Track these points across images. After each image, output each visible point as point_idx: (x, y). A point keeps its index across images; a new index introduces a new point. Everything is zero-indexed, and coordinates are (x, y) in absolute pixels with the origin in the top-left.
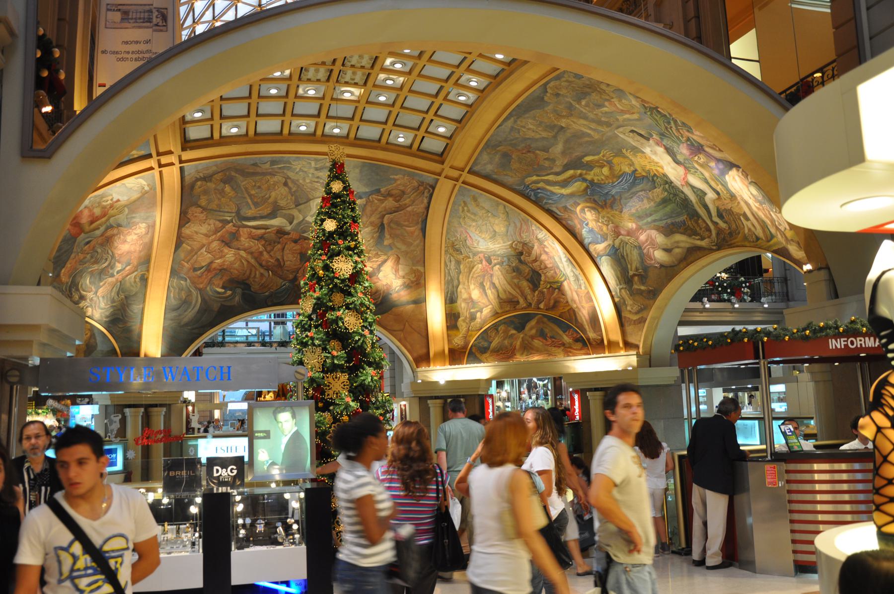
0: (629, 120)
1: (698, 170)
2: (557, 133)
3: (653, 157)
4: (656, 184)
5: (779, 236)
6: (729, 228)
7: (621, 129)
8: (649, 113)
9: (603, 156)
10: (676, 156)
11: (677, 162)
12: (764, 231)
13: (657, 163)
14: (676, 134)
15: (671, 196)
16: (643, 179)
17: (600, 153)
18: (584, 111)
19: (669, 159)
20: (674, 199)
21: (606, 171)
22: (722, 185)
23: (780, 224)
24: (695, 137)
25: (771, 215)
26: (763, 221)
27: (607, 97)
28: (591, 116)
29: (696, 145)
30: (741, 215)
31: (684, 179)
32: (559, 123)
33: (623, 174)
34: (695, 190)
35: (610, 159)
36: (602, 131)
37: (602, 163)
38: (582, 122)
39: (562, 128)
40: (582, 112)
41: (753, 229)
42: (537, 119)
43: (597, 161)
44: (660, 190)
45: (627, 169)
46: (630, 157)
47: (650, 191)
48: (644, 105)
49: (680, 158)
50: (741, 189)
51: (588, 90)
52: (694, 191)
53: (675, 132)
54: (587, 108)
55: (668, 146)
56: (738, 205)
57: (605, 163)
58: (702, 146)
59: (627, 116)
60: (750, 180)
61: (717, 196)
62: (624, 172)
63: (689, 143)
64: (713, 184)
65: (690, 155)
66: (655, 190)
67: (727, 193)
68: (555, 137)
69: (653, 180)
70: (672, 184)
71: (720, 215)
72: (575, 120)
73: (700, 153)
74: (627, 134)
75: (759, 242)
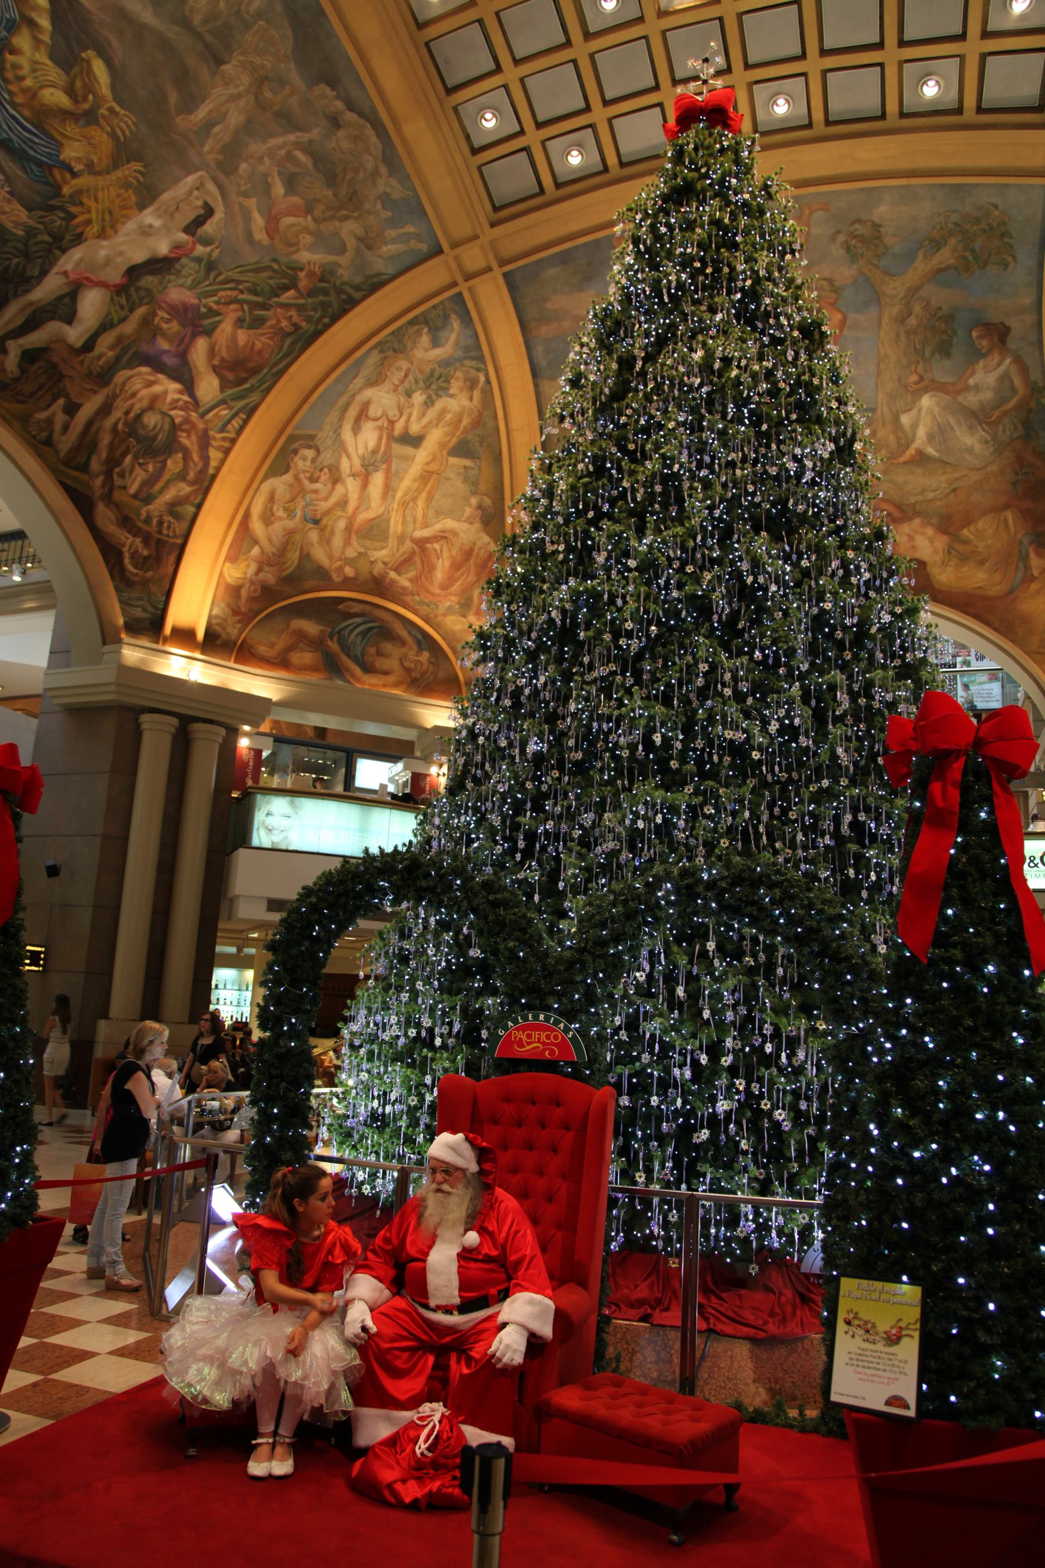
0: (247, 219)
1: (132, 310)
2: (199, 36)
3: (130, 226)
4: (43, 213)
5: (99, 481)
6: (16, 380)
7: (211, 186)
8: (276, 266)
9: (111, 110)
10: (152, 273)
11: (134, 272)
12: (77, 449)
13: (113, 227)
14: (221, 294)
15: (20, 246)
16: (50, 185)
17: (122, 106)
18: (274, 142)
19: (139, 256)
20: (14, 251)
21: (56, 97)
22: (117, 359)
23: (122, 475)
24: (226, 327)
25: (124, 455)
26: (93, 447)
27: (319, 210)
28: (256, 147)
29: (206, 322)
30: (67, 397)
31: (87, 279)
32: (234, 62)
33: (54, 139)
34: (66, 300)
35: (101, 121)
36: (202, 145)
37: (85, 99)
38: (235, 118)
39: (219, 62)
40: (272, 135)
41: (58, 427)
42: (262, 23)
43: (90, 87)
44: (26, 219)
45: (74, 154)
46: (119, 174)
47: (11, 193)
48: (302, 270)
49: (148, 281)
50: (134, 395)
51: (344, 191)
52: (60, 299)
53: (229, 293)
54: (283, 152)
55: (177, 266)
56: (89, 390)
57: (86, 106)
58: (209, 332)
59: (259, 221)
60: (172, 413)
61: (79, 344)
62: (61, 145)
63: (203, 310)
64: (106, 340)
65: (165, 302)
66: (20, 207)
67: (101, 367)
68: (185, 23)
69: (52, 209)
70: (57, 252)
71: (29, 356)
72: (242, 102)
73: (182, 324)
74: (196, 193)
75: (43, 447)
